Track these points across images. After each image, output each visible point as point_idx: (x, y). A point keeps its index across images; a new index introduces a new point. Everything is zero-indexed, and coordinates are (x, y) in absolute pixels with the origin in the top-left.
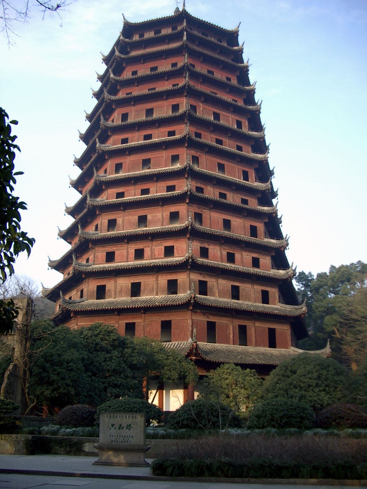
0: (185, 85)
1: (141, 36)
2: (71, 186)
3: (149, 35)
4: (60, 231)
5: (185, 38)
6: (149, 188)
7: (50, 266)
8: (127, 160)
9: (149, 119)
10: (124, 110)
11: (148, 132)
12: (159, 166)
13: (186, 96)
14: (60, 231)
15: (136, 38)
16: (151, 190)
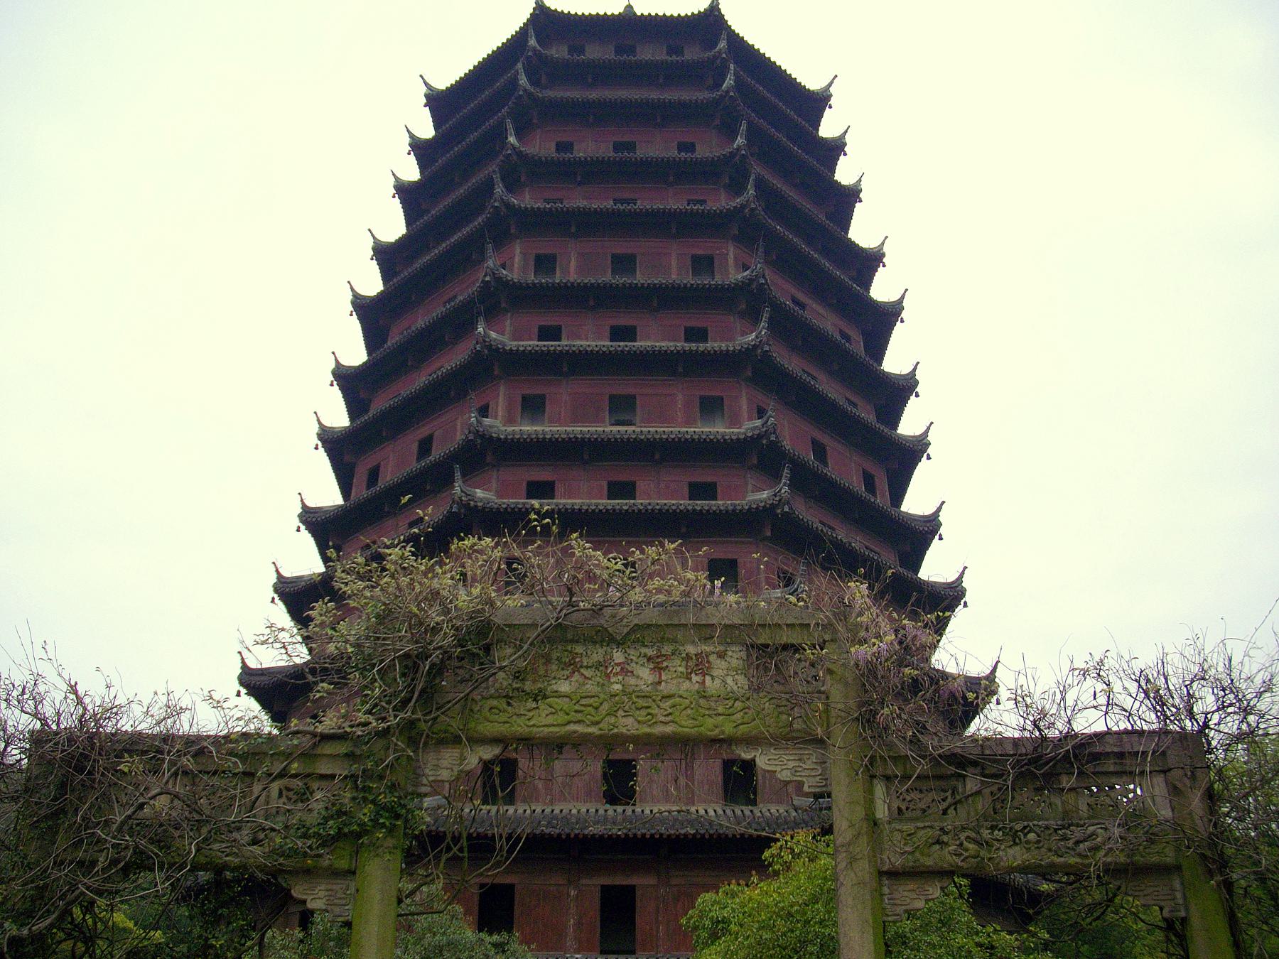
0: (743, 207)
1: (576, 49)
2: (320, 444)
3: (595, 52)
4: (279, 575)
5: (729, 81)
6: (633, 479)
7: (242, 683)
8: (563, 393)
9: (620, 280)
10: (545, 246)
11: (624, 320)
12: (665, 419)
13: (736, 239)
14: (279, 575)
15: (559, 52)
16: (641, 485)
